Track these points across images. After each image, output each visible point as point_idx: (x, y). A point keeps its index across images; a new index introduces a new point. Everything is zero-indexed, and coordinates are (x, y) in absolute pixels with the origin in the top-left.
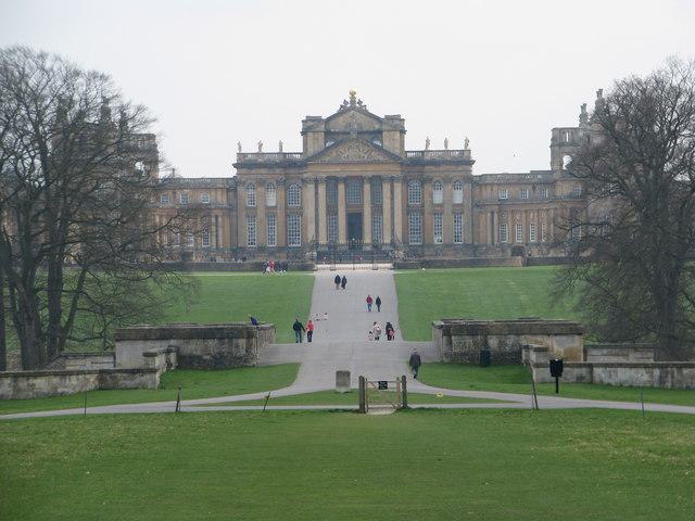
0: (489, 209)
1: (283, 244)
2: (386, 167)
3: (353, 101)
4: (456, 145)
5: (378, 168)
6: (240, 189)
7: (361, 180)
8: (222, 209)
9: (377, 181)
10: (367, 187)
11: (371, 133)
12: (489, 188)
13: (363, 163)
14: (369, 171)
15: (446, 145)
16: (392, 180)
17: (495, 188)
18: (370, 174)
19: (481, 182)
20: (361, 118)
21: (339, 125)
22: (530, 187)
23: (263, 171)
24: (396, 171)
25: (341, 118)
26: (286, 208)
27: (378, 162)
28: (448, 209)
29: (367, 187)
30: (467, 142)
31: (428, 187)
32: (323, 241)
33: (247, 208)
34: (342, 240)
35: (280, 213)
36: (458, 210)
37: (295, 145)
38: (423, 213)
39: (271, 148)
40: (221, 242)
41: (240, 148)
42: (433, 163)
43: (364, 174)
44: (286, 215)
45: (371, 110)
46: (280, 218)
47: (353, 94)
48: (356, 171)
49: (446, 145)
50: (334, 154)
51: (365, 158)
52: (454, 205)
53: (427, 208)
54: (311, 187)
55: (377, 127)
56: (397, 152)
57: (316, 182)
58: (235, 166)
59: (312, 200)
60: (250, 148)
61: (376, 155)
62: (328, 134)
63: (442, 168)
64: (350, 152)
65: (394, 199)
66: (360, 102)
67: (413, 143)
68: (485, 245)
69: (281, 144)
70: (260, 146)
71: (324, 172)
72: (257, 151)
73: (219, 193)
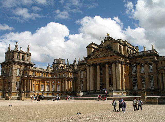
2: (112, 57)
5: (110, 58)
6: (79, 73)
9: (110, 64)
10: (107, 66)
12: (160, 63)
14: (108, 59)
15: (144, 49)
18: (107, 61)
27: (110, 56)
42: (140, 56)
48: (102, 60)
49: (144, 49)
50: (95, 55)
57: (89, 66)
63: (143, 58)
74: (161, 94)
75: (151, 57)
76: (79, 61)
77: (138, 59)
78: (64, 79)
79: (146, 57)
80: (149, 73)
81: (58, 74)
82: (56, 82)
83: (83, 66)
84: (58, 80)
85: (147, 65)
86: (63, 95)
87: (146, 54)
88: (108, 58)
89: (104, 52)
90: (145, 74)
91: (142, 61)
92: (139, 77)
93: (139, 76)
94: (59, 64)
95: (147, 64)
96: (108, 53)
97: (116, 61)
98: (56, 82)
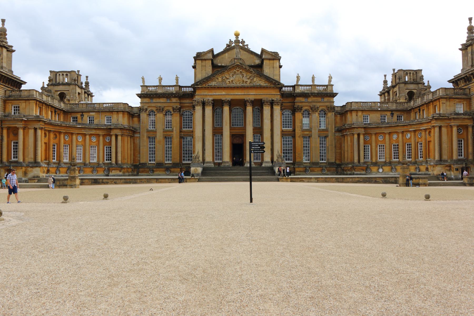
0: (356, 131)
1: (177, 161)
3: (237, 41)
4: (322, 80)
6: (144, 116)
7: (243, 104)
8: (121, 129)
9: (259, 104)
10: (249, 109)
11: (251, 66)
12: (354, 114)
13: (248, 88)
14: (252, 95)
15: (313, 81)
16: (272, 103)
17: (360, 113)
18: (252, 98)
19: (344, 111)
20: (244, 56)
21: (225, 61)
22: (389, 114)
23: (162, 100)
24: (275, 95)
25: (227, 54)
26: (181, 131)
27: (260, 87)
28: (315, 133)
29: (249, 109)
30: (330, 78)
31: (298, 115)
32: (209, 158)
33: (148, 131)
34: (227, 157)
35: (176, 134)
36: (323, 135)
37: (188, 79)
38: (294, 137)
39: (169, 81)
40: (120, 158)
41: (143, 81)
42: (304, 95)
43: (246, 98)
44: (181, 138)
45: (252, 49)
46: (176, 140)
47: (237, 35)
49: (313, 81)
50: (220, 79)
51: (248, 84)
52: (319, 131)
53: (298, 132)
54: (199, 109)
55: (257, 62)
56: (276, 78)
57: (204, 104)
58: (140, 96)
59: (202, 120)
60: (152, 81)
61: (258, 81)
62: (214, 66)
63: (310, 100)
64: (235, 78)
65: (275, 121)
66: (243, 42)
67: (287, 78)
68: (353, 163)
69: (177, 79)
70: (160, 79)
71: (210, 95)
72: (157, 84)
73: (121, 115)
74: (356, 173)
75: (326, 99)
76: (142, 84)
77: (298, 99)
78: (113, 132)
79: (315, 98)
80: (319, 131)
81: (86, 115)
82: (88, 137)
83: (158, 100)
84: (93, 132)
85: (317, 114)
86: (114, 172)
87: (316, 92)
88: (253, 92)
89: (245, 76)
90: (313, 131)
91: (307, 104)
92: (299, 137)
93: (298, 136)
94: (71, 87)
95: (317, 111)
96: (255, 79)
97: (272, 100)
98: (88, 137)
